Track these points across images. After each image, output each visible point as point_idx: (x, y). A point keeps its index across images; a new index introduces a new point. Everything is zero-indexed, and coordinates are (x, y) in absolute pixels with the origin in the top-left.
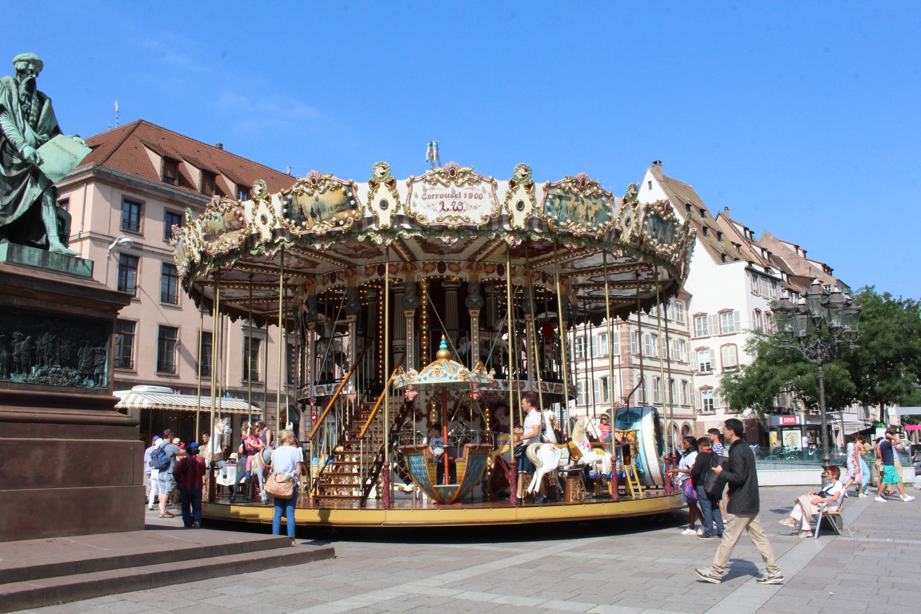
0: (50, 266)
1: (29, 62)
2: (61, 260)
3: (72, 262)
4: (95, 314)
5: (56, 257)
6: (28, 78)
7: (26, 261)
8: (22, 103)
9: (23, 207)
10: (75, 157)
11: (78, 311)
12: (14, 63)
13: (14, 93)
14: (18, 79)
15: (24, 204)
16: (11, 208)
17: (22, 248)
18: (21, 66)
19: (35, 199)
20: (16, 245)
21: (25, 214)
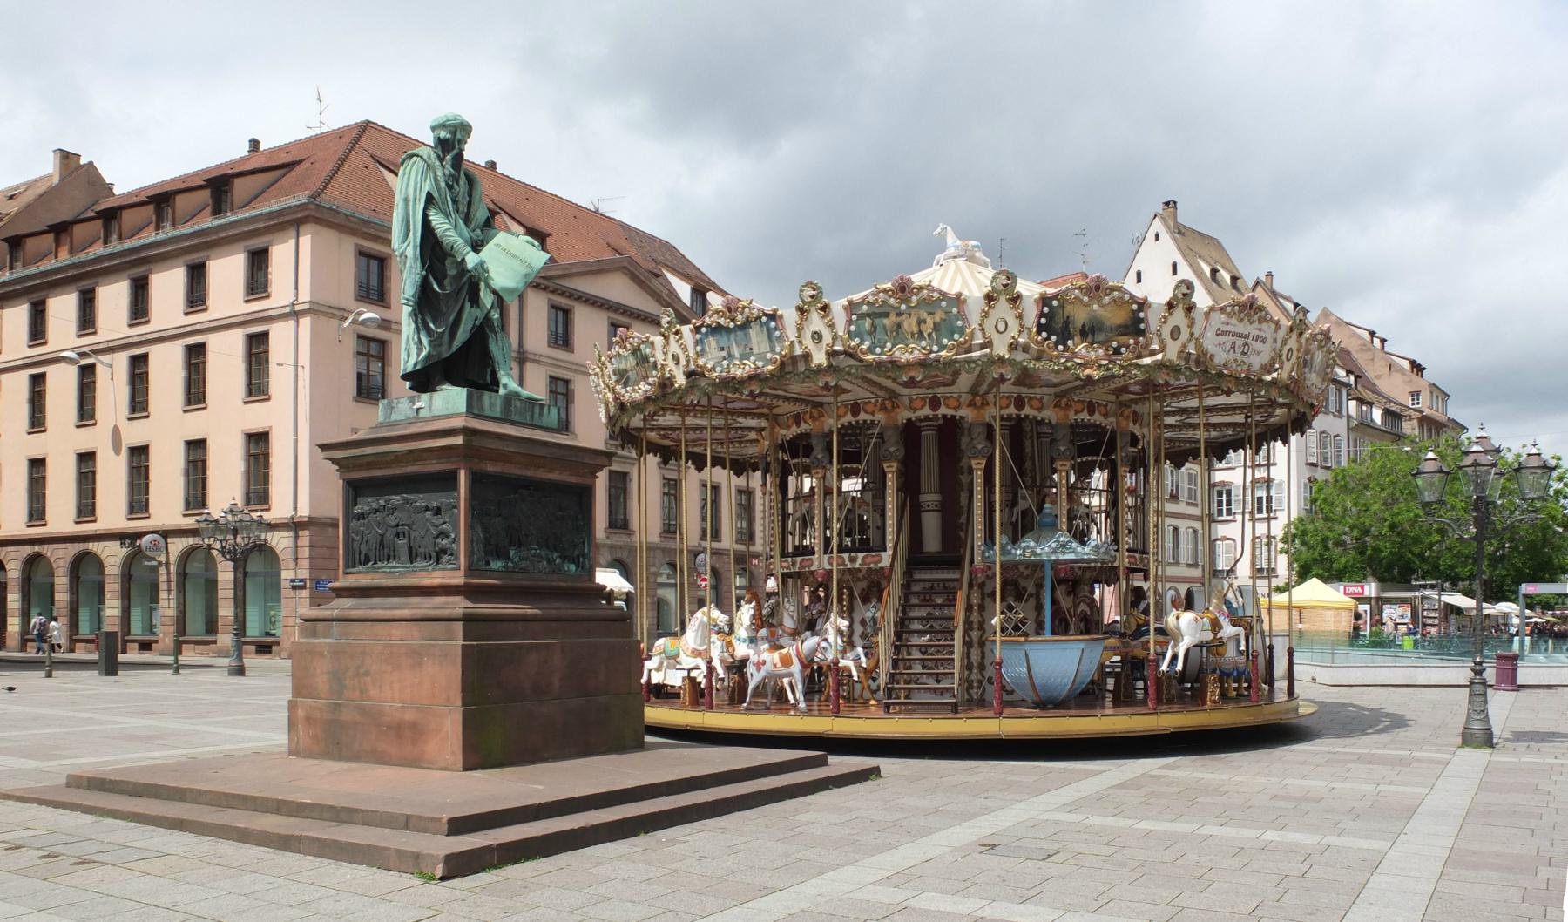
0: (515, 418)
3: (537, 409)
4: (573, 480)
5: (519, 404)
7: (488, 412)
8: (450, 187)
9: (462, 335)
10: (530, 266)
11: (554, 476)
13: (439, 173)
21: (467, 345)
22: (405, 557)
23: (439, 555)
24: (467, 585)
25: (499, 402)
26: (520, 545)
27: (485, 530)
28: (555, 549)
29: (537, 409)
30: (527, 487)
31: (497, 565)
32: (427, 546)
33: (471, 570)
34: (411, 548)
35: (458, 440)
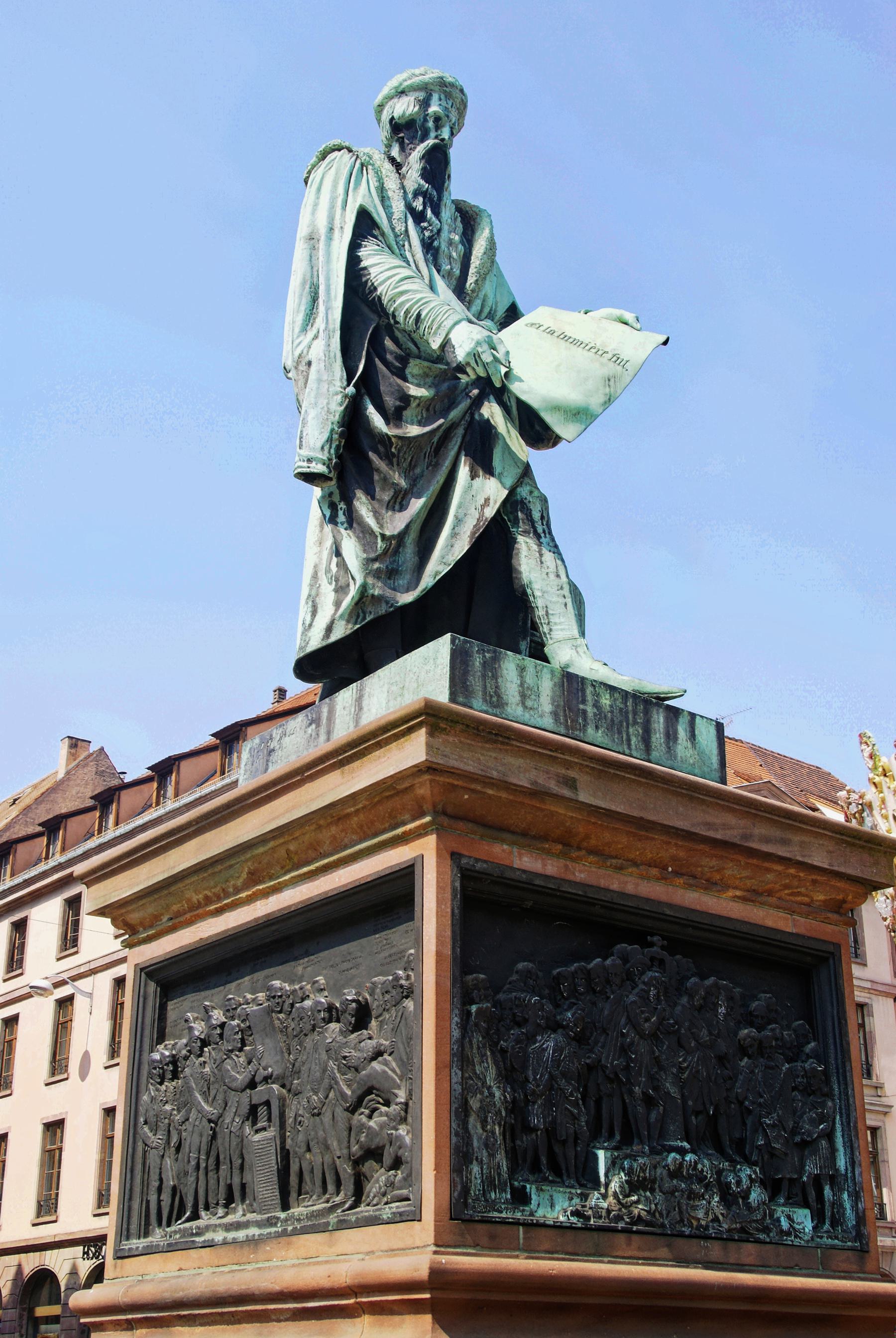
1: (426, 91)
2: (624, 712)
3: (659, 720)
5: (606, 701)
6: (430, 142)
8: (419, 217)
9: (450, 548)
10: (616, 359)
12: (381, 106)
14: (395, 152)
15: (454, 535)
16: (409, 552)
17: (496, 659)
18: (405, 107)
19: (490, 512)
20: (476, 645)
22: (265, 1185)
23: (360, 1175)
24: (439, 1279)
25: (547, 686)
26: (626, 1137)
27: (511, 1074)
28: (740, 1152)
29: (659, 720)
30: (640, 938)
31: (555, 1207)
32: (327, 1142)
33: (464, 1217)
34: (285, 1155)
35: (413, 751)
